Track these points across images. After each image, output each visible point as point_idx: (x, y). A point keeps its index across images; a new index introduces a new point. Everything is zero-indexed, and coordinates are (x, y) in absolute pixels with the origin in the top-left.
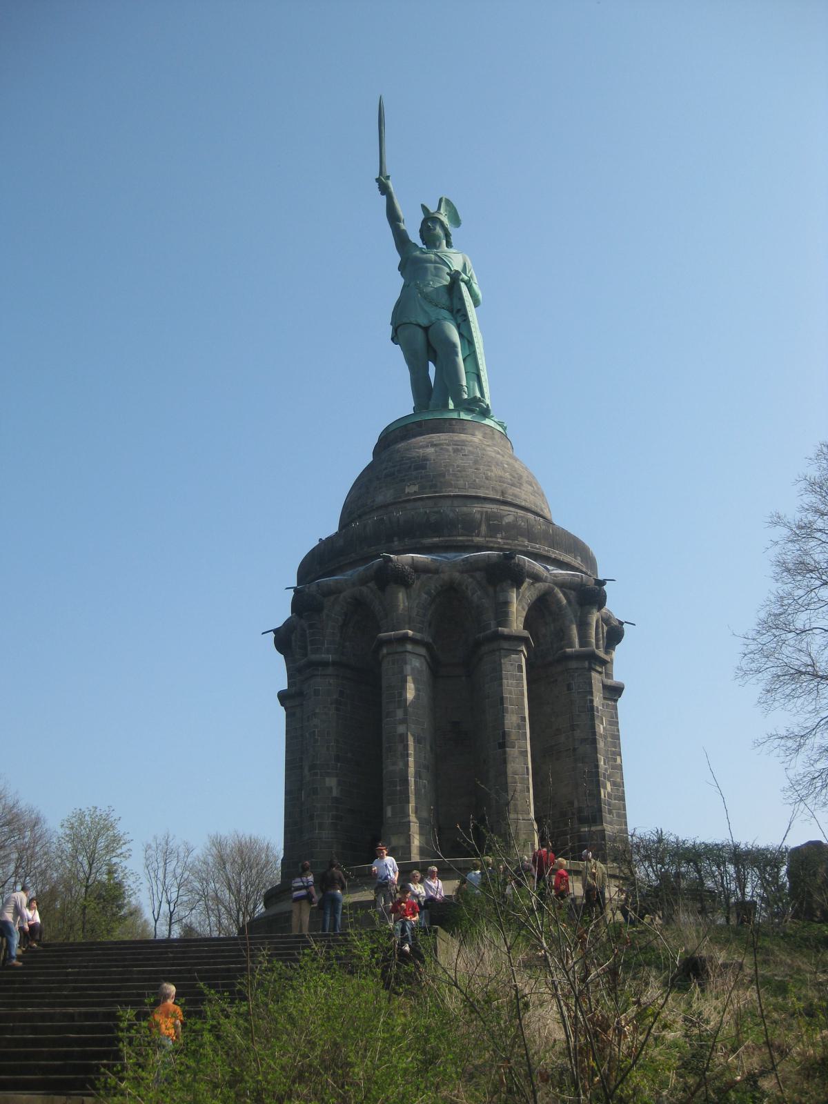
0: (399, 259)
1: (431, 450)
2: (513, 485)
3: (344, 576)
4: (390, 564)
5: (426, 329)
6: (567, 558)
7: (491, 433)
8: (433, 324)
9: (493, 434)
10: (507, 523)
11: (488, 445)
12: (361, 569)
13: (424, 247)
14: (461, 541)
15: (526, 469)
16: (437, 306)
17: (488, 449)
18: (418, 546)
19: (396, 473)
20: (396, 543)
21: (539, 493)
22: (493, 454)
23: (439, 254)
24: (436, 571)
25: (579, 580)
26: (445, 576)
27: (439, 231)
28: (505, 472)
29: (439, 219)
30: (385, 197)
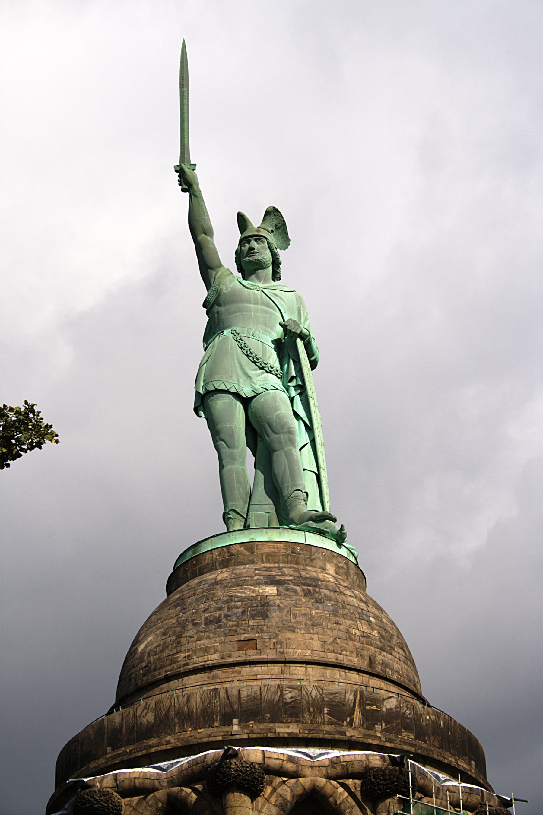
0: (203, 293)
1: (271, 590)
2: (382, 649)
3: (155, 768)
4: (234, 761)
5: (246, 402)
6: (462, 764)
7: (345, 567)
8: (258, 394)
9: (348, 568)
10: (387, 709)
11: (345, 587)
12: (184, 761)
13: (240, 275)
14: (329, 733)
15: (393, 623)
16: (262, 368)
17: (348, 593)
18: (269, 735)
19: (224, 620)
20: (236, 728)
21: (409, 660)
22: (355, 602)
23: (265, 291)
24: (295, 775)
25: (479, 797)
26: (306, 782)
27: (267, 257)
28: (373, 630)
29: (266, 238)
30: (187, 194)
